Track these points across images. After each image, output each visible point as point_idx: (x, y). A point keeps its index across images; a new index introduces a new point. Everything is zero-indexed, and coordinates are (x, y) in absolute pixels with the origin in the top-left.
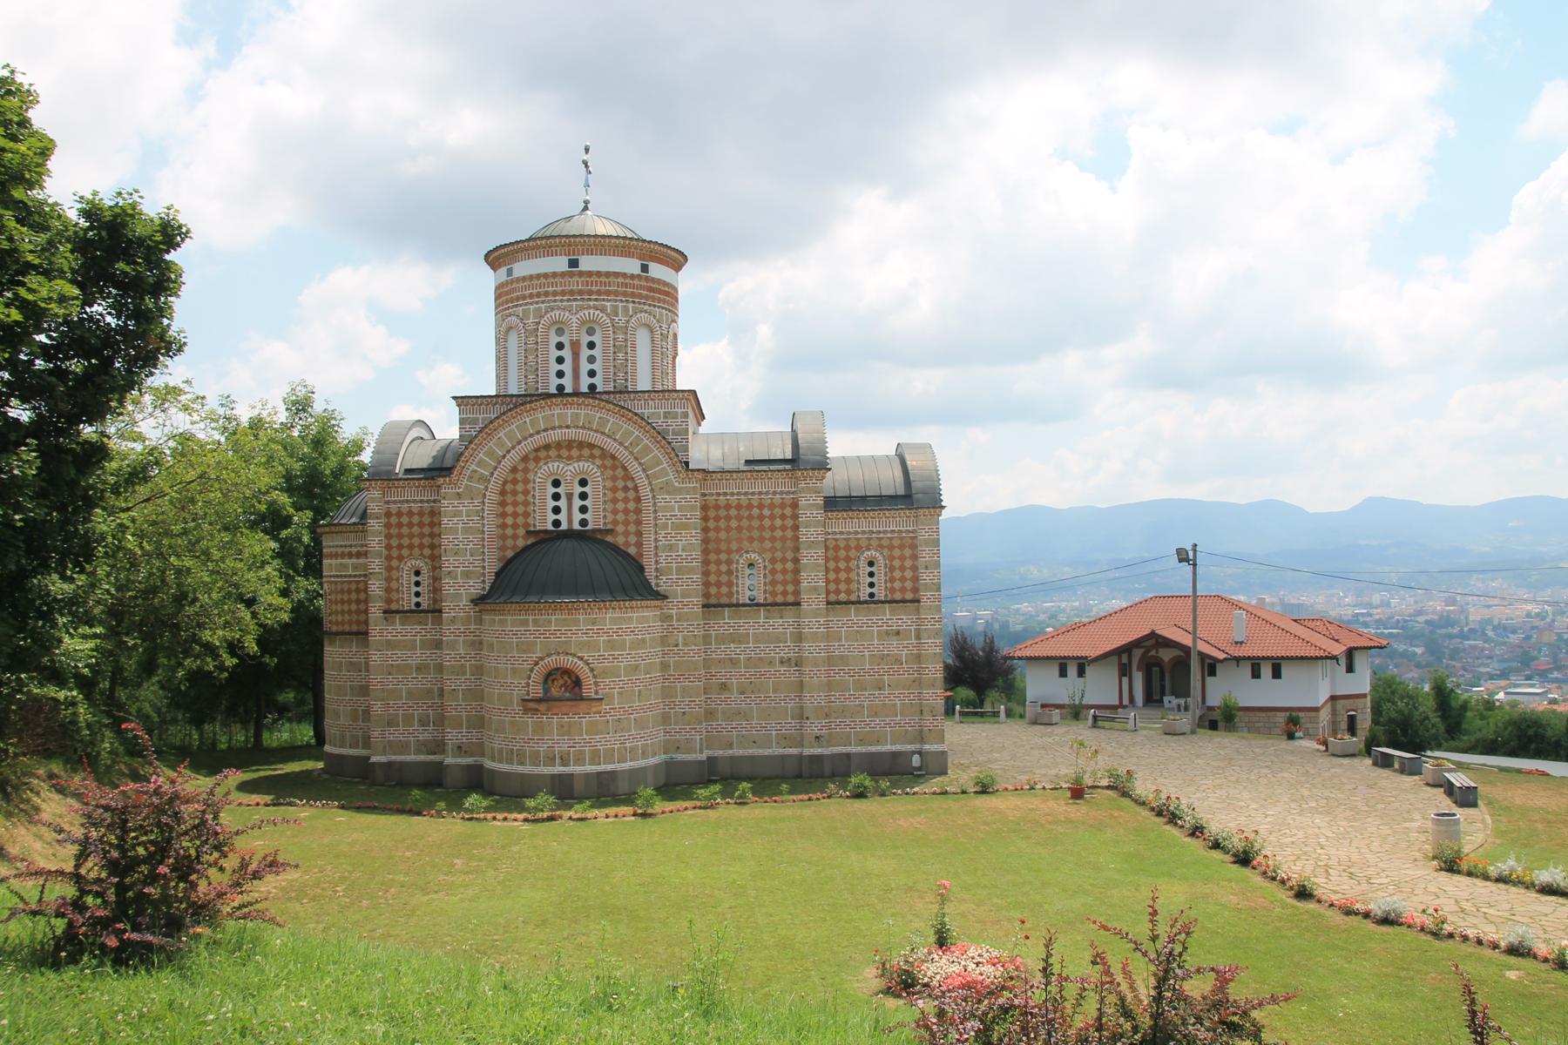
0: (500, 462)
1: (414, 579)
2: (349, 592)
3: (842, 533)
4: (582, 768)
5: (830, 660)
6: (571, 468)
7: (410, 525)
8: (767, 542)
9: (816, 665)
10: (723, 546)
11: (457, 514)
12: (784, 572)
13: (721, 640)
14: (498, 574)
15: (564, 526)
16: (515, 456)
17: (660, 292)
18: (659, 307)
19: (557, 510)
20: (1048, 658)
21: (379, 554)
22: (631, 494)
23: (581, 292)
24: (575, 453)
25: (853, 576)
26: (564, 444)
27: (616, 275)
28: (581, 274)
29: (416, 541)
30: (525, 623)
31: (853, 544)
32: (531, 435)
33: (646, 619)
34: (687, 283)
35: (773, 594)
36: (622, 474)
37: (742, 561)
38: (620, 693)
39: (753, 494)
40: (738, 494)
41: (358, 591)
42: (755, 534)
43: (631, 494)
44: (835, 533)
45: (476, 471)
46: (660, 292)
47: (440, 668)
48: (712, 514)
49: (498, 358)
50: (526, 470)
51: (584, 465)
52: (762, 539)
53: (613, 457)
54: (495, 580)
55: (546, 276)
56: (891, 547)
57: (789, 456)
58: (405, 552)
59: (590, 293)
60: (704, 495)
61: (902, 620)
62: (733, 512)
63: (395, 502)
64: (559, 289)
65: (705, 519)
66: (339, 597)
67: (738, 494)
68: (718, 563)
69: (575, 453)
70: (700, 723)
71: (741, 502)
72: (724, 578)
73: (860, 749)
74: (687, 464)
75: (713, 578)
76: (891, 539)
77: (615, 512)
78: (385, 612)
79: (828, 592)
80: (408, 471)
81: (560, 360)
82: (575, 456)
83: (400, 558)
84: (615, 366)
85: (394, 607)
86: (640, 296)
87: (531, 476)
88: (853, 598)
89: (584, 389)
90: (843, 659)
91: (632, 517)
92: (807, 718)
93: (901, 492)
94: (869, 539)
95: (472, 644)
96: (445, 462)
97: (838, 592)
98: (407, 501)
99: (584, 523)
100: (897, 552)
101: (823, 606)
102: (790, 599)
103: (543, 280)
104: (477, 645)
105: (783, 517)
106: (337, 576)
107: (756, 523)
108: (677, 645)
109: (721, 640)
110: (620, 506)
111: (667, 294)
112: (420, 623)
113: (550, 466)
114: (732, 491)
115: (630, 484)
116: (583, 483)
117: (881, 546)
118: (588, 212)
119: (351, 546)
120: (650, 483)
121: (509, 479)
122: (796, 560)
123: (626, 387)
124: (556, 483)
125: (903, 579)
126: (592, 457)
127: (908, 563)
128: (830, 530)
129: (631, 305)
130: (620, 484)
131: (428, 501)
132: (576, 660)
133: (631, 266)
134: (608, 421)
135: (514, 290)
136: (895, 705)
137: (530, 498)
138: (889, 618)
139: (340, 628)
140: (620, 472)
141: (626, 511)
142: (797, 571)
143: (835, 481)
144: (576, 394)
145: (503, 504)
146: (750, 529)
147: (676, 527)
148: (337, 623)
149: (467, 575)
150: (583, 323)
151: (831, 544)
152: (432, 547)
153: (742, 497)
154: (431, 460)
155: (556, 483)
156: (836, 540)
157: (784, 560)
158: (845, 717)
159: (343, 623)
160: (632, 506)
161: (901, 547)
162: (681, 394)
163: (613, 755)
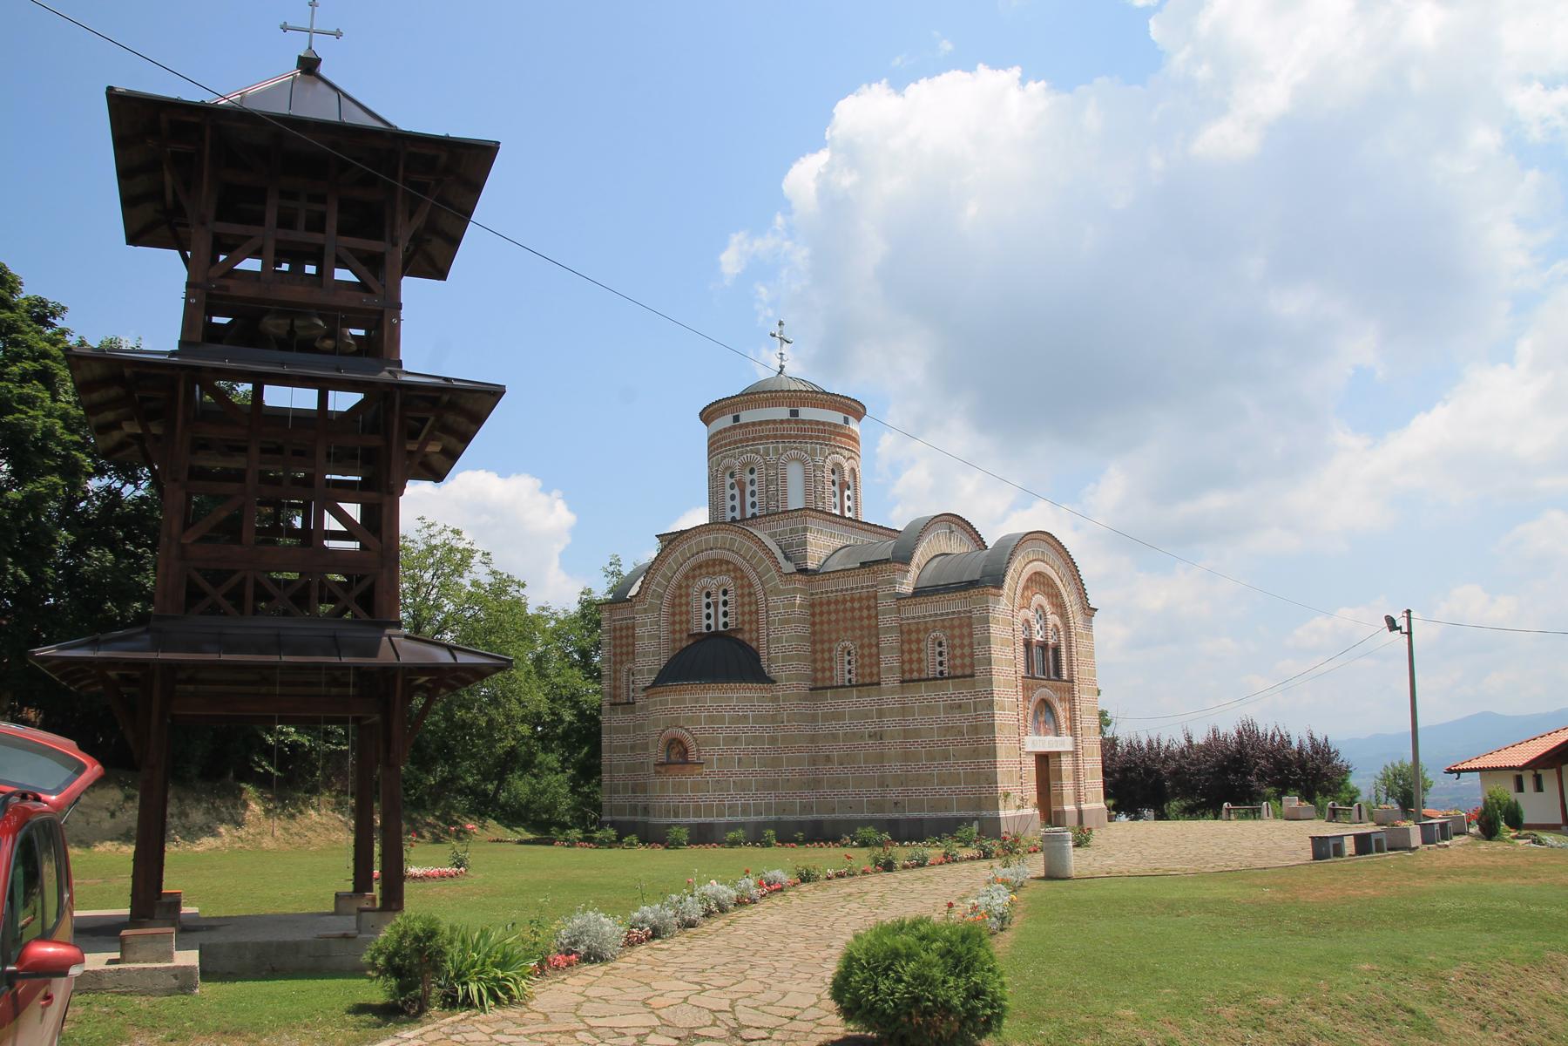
0: (669, 582)
3: (914, 618)
9: (893, 738)
10: (826, 637)
11: (644, 625)
13: (826, 718)
15: (713, 629)
19: (708, 616)
20: (1497, 769)
23: (741, 441)
25: (923, 656)
26: (710, 563)
27: (767, 422)
33: (750, 699)
35: (863, 676)
38: (719, 760)
39: (847, 590)
40: (837, 591)
42: (849, 624)
44: (908, 618)
50: (688, 586)
51: (724, 578)
52: (853, 629)
56: (952, 627)
59: (748, 440)
60: (812, 594)
62: (833, 607)
63: (618, 620)
67: (837, 591)
69: (717, 569)
73: (933, 815)
76: (952, 619)
79: (903, 672)
83: (622, 663)
84: (767, 497)
85: (618, 701)
86: (790, 436)
88: (924, 676)
90: (917, 733)
92: (887, 786)
97: (911, 671)
98: (626, 619)
99: (725, 625)
100: (957, 632)
105: (868, 608)
107: (849, 615)
109: (826, 718)
114: (830, 587)
116: (725, 593)
117: (944, 627)
124: (708, 595)
126: (728, 571)
127: (966, 642)
128: (904, 616)
132: (683, 732)
133: (782, 413)
136: (959, 774)
137: (689, 608)
144: (743, 520)
146: (845, 620)
147: (783, 622)
150: (744, 465)
151: (905, 629)
156: (909, 624)
157: (870, 646)
158: (919, 785)
161: (961, 626)
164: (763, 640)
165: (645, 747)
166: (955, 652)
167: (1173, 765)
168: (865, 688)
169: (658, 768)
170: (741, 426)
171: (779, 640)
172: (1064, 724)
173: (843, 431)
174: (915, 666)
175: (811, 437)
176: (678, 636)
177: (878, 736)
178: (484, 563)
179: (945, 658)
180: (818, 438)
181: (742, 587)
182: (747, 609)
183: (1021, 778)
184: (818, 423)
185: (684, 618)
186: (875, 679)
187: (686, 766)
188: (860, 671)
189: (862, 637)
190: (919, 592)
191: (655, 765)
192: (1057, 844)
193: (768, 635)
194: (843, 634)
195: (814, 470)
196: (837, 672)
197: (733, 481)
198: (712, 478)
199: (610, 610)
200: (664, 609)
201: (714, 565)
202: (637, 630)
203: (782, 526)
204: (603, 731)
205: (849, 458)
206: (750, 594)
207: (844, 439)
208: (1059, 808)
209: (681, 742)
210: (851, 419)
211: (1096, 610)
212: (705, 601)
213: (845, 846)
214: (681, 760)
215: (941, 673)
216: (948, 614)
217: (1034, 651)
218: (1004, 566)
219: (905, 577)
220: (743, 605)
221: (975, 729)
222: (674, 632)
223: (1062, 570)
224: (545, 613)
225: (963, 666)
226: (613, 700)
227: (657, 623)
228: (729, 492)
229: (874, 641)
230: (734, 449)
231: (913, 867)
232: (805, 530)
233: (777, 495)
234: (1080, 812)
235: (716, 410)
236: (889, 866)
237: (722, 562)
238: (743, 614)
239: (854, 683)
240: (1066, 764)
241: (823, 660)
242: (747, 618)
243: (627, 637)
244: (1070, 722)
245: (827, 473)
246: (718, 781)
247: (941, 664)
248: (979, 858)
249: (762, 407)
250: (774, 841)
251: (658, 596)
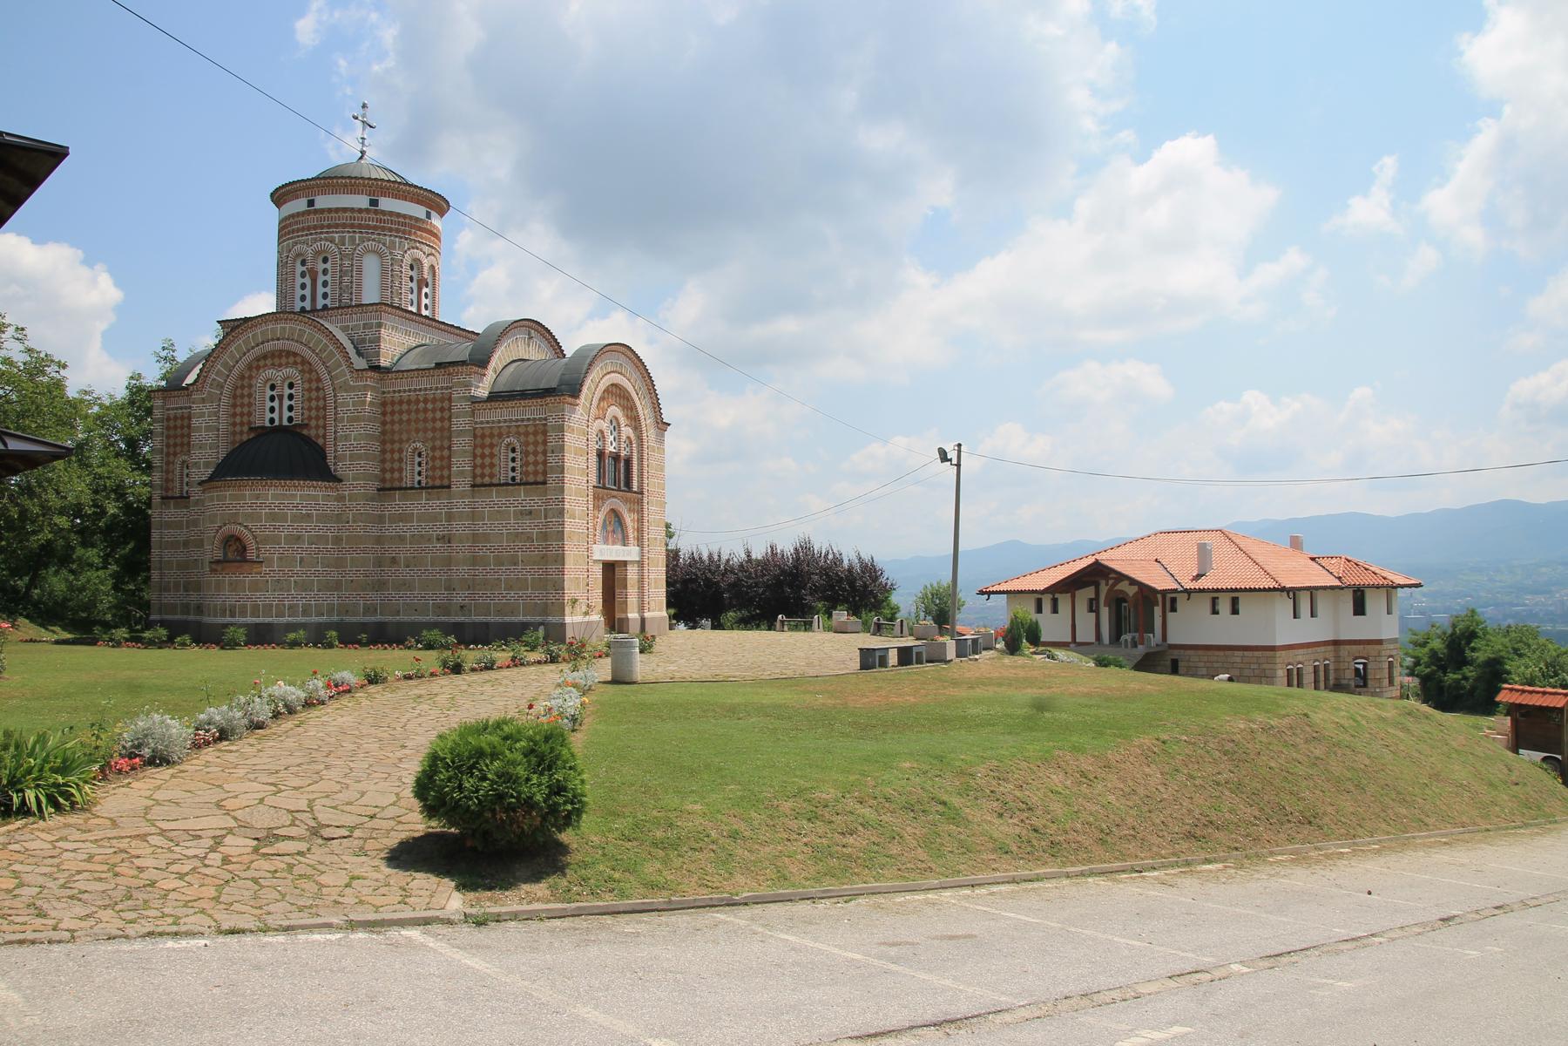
3: (488, 422)
4: (244, 619)
6: (281, 373)
9: (461, 542)
10: (396, 437)
13: (394, 519)
15: (277, 423)
19: (272, 410)
23: (315, 227)
25: (496, 461)
26: (277, 354)
27: (345, 210)
31: (496, 432)
33: (315, 498)
38: (280, 559)
39: (420, 390)
40: (410, 391)
42: (421, 425)
44: (482, 423)
50: (251, 377)
52: (425, 430)
56: (527, 434)
59: (322, 227)
60: (384, 393)
62: (405, 407)
63: (173, 409)
69: (284, 360)
71: (411, 397)
76: (526, 426)
79: (474, 477)
81: (303, 286)
83: (175, 454)
84: (340, 288)
85: (170, 494)
86: (368, 227)
88: (495, 481)
90: (486, 538)
92: (454, 589)
97: (483, 476)
99: (290, 419)
100: (531, 439)
105: (442, 410)
107: (421, 416)
109: (394, 519)
114: (403, 386)
116: (291, 386)
121: (239, 385)
124: (273, 387)
126: (295, 363)
127: (540, 448)
133: (362, 201)
136: (526, 579)
137: (252, 400)
138: (524, 499)
144: (314, 310)
147: (352, 420)
150: (317, 253)
151: (479, 433)
156: (483, 428)
161: (535, 433)
163: (272, 610)
164: (330, 436)
165: (200, 544)
166: (529, 459)
167: (732, 578)
168: (436, 490)
169: (214, 566)
170: (316, 211)
171: (347, 438)
172: (632, 534)
173: (425, 226)
174: (487, 471)
175: (390, 230)
176: (238, 429)
177: (447, 539)
178: (18, 339)
179: (518, 464)
180: (398, 231)
181: (310, 381)
182: (314, 404)
183: (588, 585)
184: (398, 215)
185: (246, 410)
186: (446, 482)
188: (430, 473)
189: (434, 439)
190: (494, 397)
191: (211, 562)
192: (624, 650)
193: (335, 432)
194: (415, 435)
195: (392, 264)
196: (407, 474)
197: (304, 268)
198: (282, 265)
199: (164, 398)
200: (225, 400)
201: (280, 357)
202: (194, 421)
203: (356, 320)
204: (153, 526)
205: (428, 255)
206: (318, 389)
207: (424, 234)
208: (623, 616)
209: (238, 539)
210: (433, 213)
211: (669, 425)
212: (269, 393)
213: (409, 648)
214: (238, 558)
215: (513, 479)
216: (523, 420)
217: (607, 461)
218: (582, 376)
219: (481, 381)
220: (310, 400)
221: (544, 536)
222: (234, 424)
223: (639, 384)
224: (87, 397)
225: (536, 473)
226: (164, 494)
227: (216, 414)
228: (299, 281)
229: (446, 444)
230: (307, 235)
231: (481, 670)
232: (380, 325)
233: (352, 288)
234: (643, 620)
235: (289, 192)
236: (457, 669)
237: (289, 353)
238: (310, 409)
239: (424, 485)
240: (632, 573)
241: (393, 461)
242: (314, 413)
243: (182, 427)
244: (638, 532)
245: (406, 268)
246: (278, 581)
247: (513, 469)
248: (546, 662)
249: (340, 193)
250: (337, 643)
251: (218, 385)
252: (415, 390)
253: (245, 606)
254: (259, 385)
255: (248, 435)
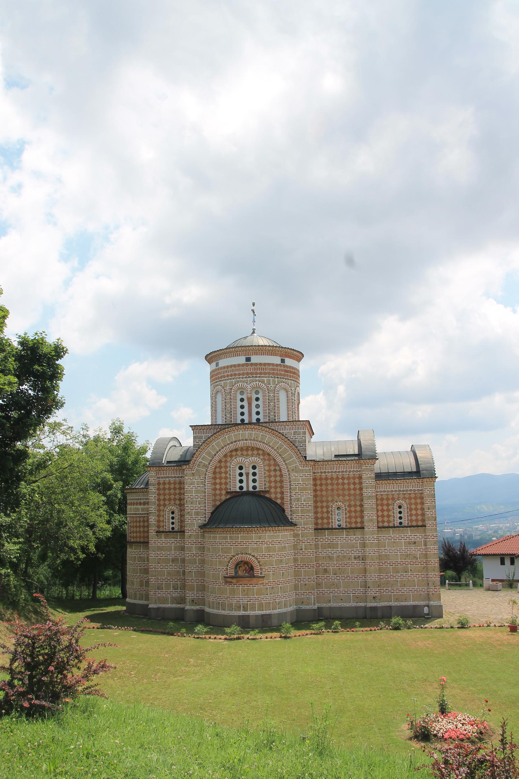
1: (171, 515)
2: (140, 522)
3: (384, 491)
4: (254, 612)
5: (380, 557)
6: (248, 460)
7: (170, 489)
8: (347, 496)
10: (324, 499)
12: (355, 511)
13: (324, 547)
14: (212, 513)
15: (245, 489)
16: (221, 454)
17: (290, 372)
18: (290, 380)
19: (241, 481)
20: (494, 555)
21: (154, 503)
22: (278, 473)
23: (252, 374)
24: (250, 452)
25: (391, 513)
26: (244, 448)
27: (269, 364)
28: (252, 364)
29: (172, 497)
30: (226, 538)
32: (228, 444)
34: (303, 366)
35: (350, 523)
36: (273, 463)
37: (334, 506)
38: (273, 574)
39: (339, 472)
40: (332, 472)
41: (144, 521)
42: (341, 492)
43: (278, 473)
44: (381, 491)
45: (202, 462)
46: (290, 372)
47: (183, 561)
48: (318, 482)
49: (212, 407)
50: (226, 462)
52: (344, 495)
53: (269, 455)
54: (211, 516)
55: (235, 366)
56: (410, 498)
57: (356, 452)
58: (167, 502)
59: (257, 374)
60: (314, 473)
61: (417, 536)
62: (329, 481)
63: (162, 478)
64: (241, 372)
65: (315, 485)
66: (135, 524)
68: (322, 507)
69: (250, 452)
70: (314, 590)
71: (333, 476)
72: (325, 515)
74: (305, 457)
75: (319, 515)
76: (410, 494)
77: (270, 482)
78: (157, 532)
79: (378, 522)
80: (168, 462)
81: (242, 407)
82: (250, 454)
83: (165, 505)
84: (269, 409)
85: (161, 529)
86: (281, 374)
87: (228, 464)
88: (391, 525)
89: (254, 421)
91: (279, 485)
92: (369, 587)
93: (414, 470)
94: (399, 494)
95: (200, 548)
96: (186, 457)
97: (383, 522)
98: (168, 477)
99: (254, 487)
100: (413, 501)
101: (376, 529)
102: (359, 525)
103: (233, 368)
104: (202, 549)
105: (354, 484)
106: (134, 514)
107: (341, 487)
108: (301, 549)
110: (273, 479)
111: (294, 373)
112: (174, 538)
113: (238, 459)
115: (277, 468)
116: (254, 467)
117: (405, 498)
118: (255, 334)
119: (141, 499)
120: (287, 467)
121: (218, 466)
122: (361, 506)
123: (275, 419)
124: (241, 468)
125: (417, 515)
126: (258, 454)
129: (276, 379)
130: (272, 468)
131: (178, 477)
132: (251, 557)
133: (276, 360)
134: (266, 437)
135: (219, 373)
136: (414, 581)
137: (228, 475)
138: (410, 534)
139: (135, 540)
140: (272, 462)
141: (276, 482)
142: (362, 511)
143: (381, 465)
144: (250, 423)
145: (215, 478)
146: (338, 490)
147: (301, 489)
148: (133, 537)
149: (197, 514)
150: (253, 388)
151: (379, 497)
152: (180, 499)
153: (334, 474)
154: (180, 457)
155: (241, 468)
156: (382, 495)
157: (355, 506)
159: (136, 537)
160: (278, 479)
161: (415, 498)
162: (302, 423)
163: (270, 606)
164: (287, 498)
187: (253, 578)
209: (246, 563)
216: (407, 490)
249: (265, 355)
252: (335, 472)
253: (254, 604)
254: (232, 466)
255: (226, 496)
